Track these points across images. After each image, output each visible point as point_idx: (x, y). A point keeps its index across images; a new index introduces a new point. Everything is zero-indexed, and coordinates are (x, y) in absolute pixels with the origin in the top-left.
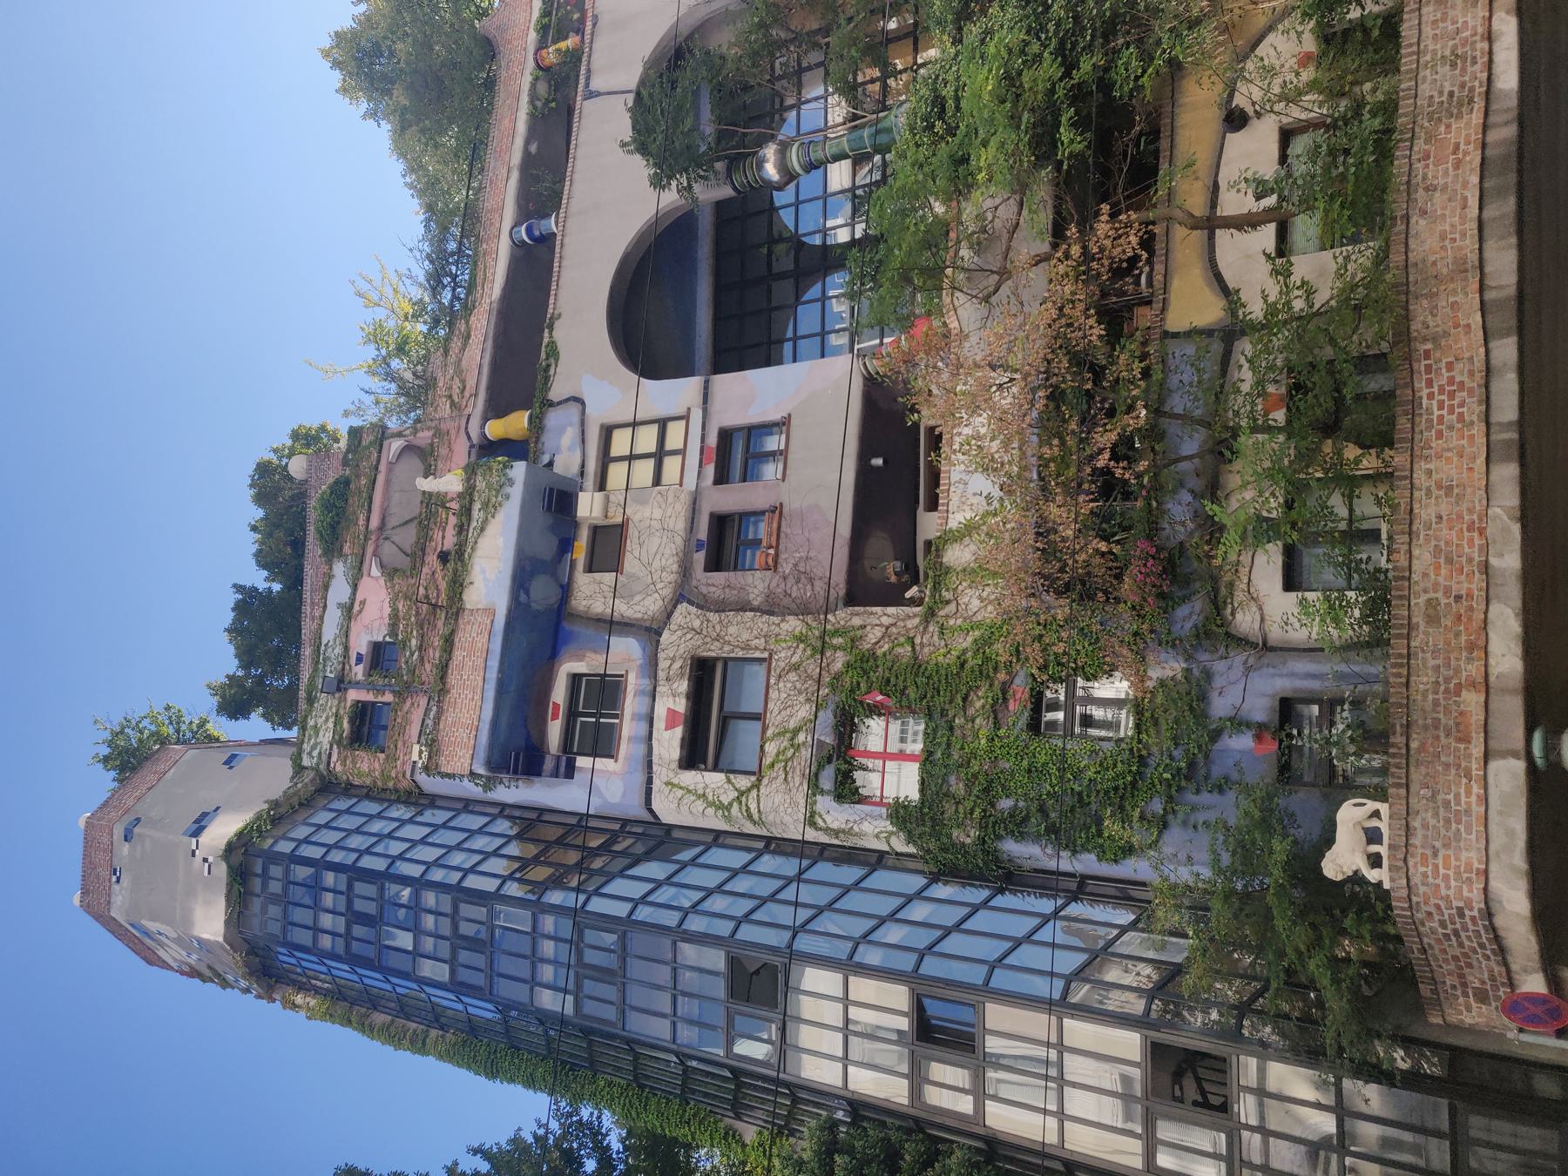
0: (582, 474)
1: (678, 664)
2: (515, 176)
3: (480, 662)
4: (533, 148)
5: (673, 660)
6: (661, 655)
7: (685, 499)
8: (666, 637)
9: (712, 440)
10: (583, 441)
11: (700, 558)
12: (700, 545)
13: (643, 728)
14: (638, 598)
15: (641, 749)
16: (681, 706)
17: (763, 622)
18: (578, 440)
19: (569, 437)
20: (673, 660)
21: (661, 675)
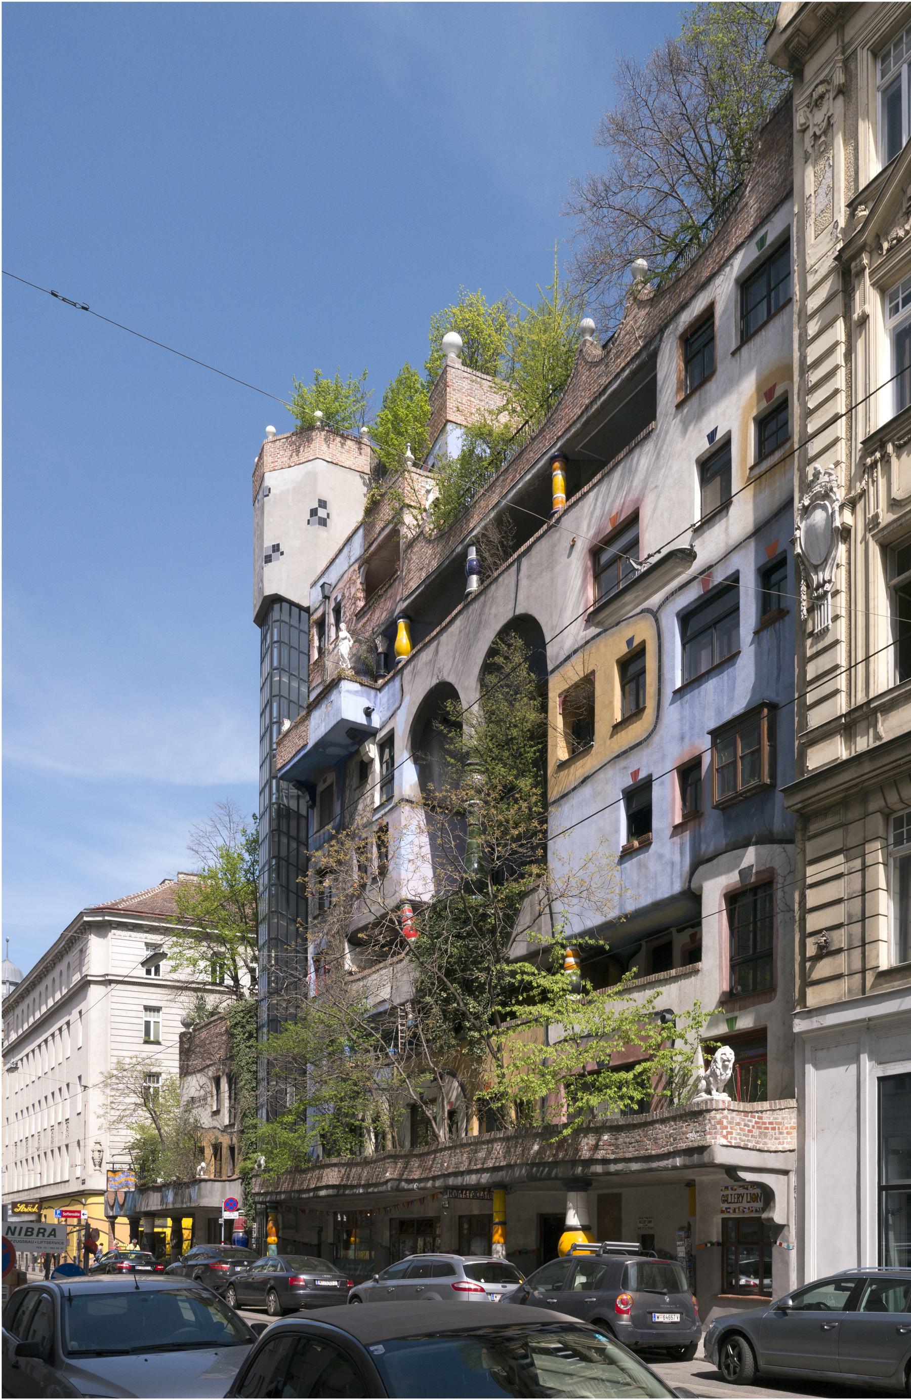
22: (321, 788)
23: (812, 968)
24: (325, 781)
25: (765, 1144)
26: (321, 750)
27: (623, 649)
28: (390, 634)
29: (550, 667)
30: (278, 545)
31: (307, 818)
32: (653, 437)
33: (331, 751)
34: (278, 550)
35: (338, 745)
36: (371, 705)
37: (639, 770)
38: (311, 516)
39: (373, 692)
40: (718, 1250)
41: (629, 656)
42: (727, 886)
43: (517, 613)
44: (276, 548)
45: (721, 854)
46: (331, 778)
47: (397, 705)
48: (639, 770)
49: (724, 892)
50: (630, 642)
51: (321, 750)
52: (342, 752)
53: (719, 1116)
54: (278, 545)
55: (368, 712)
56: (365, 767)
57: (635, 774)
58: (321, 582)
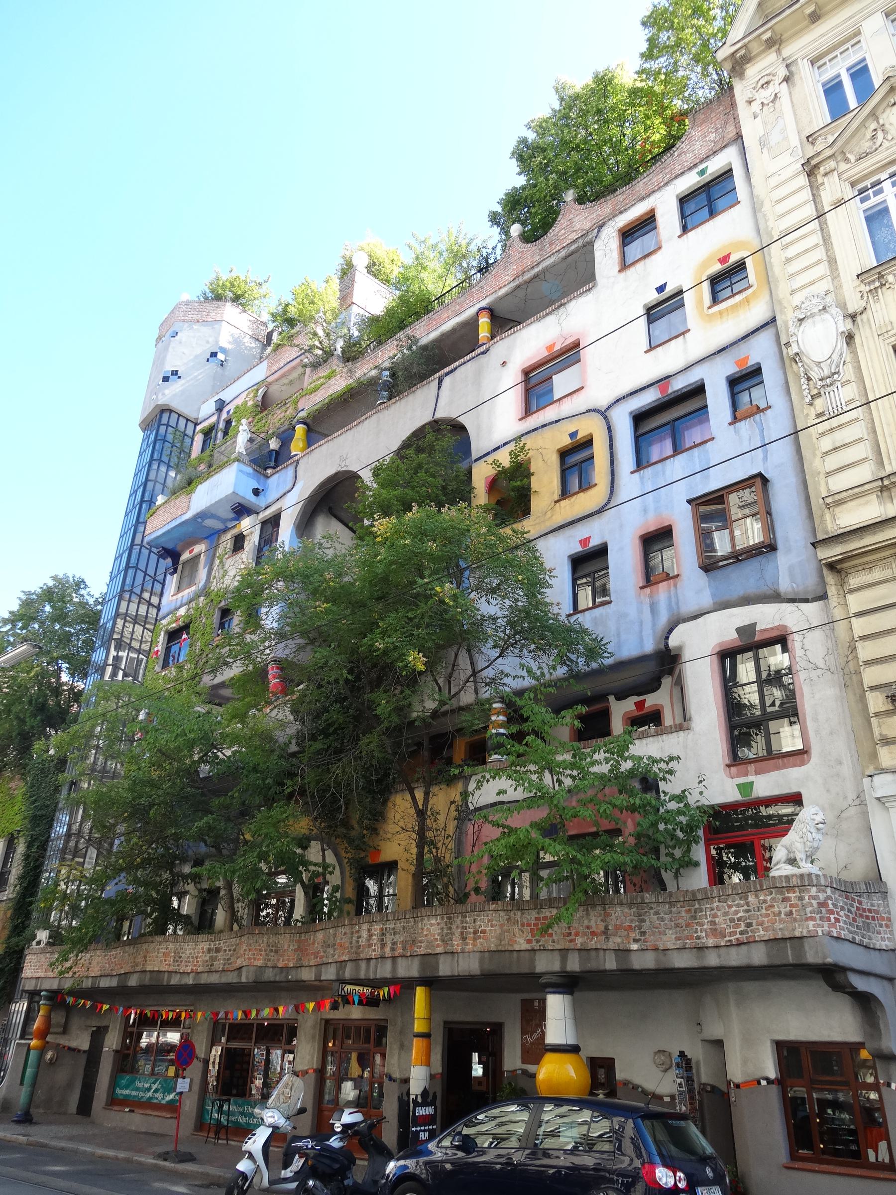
22: (185, 556)
24: (191, 552)
25: (870, 938)
26: (199, 520)
27: (566, 441)
28: (286, 438)
29: (474, 456)
30: (177, 371)
31: (163, 584)
32: (594, 291)
33: (210, 523)
34: (176, 374)
35: (218, 518)
36: (261, 488)
37: (589, 538)
38: (211, 356)
39: (262, 477)
40: (774, 1089)
41: (570, 447)
42: (720, 644)
43: (439, 415)
44: (175, 373)
45: (708, 613)
46: (200, 548)
47: (288, 488)
48: (589, 538)
49: (718, 649)
50: (573, 435)
51: (199, 520)
52: (219, 526)
53: (822, 896)
54: (177, 371)
55: (256, 492)
56: (239, 542)
57: (585, 542)
58: (216, 398)
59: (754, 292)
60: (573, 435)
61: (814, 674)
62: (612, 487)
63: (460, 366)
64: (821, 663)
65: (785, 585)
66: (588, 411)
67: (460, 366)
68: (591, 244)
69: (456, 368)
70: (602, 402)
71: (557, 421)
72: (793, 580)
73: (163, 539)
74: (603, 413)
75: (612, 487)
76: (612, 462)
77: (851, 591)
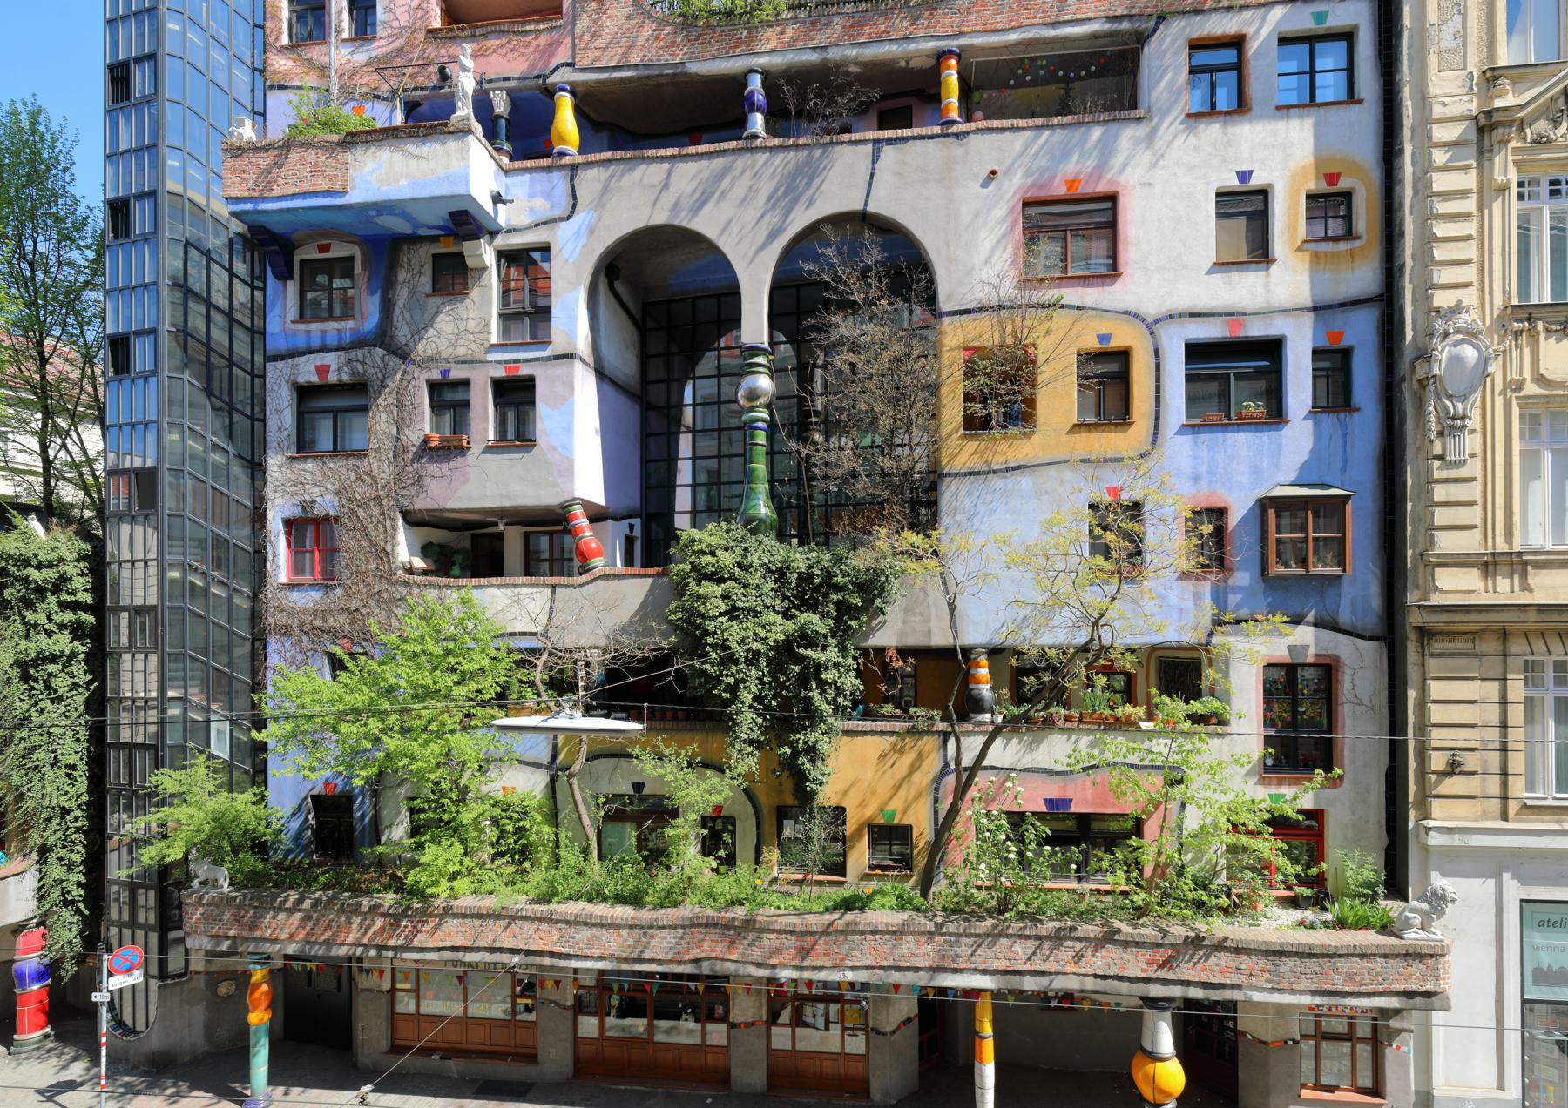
0: (509, 231)
1: (360, 368)
2: (814, 57)
3: (307, 187)
4: (853, 69)
5: (363, 363)
6: (366, 350)
7: (479, 356)
8: (379, 351)
9: (525, 371)
10: (537, 225)
11: (436, 375)
12: (446, 372)
13: (316, 342)
14: (408, 316)
15: (301, 343)
16: (332, 378)
17: (388, 444)
18: (539, 219)
19: (543, 208)
20: (363, 363)
21: (352, 353)
23: (1438, 783)
55: (497, 199)
59: (1361, 248)
60: (1103, 338)
61: (1358, 709)
62: (1156, 434)
63: (914, 138)
64: (1366, 701)
65: (1345, 618)
66: (1125, 313)
67: (914, 138)
68: (1142, 38)
69: (907, 139)
70: (1151, 309)
71: (1078, 308)
72: (1353, 613)
73: (275, 218)
74: (1152, 326)
75: (1156, 434)
76: (1158, 400)
77: (1432, 655)
